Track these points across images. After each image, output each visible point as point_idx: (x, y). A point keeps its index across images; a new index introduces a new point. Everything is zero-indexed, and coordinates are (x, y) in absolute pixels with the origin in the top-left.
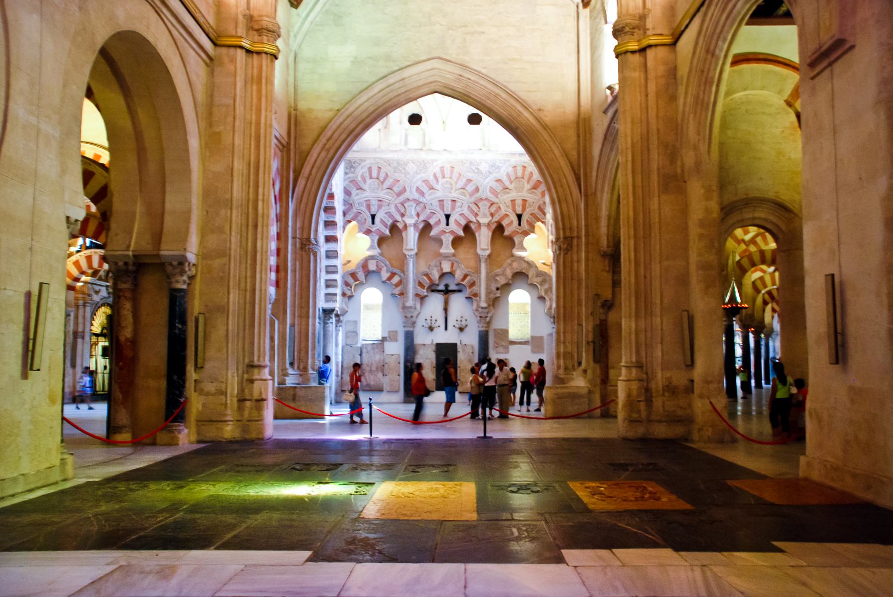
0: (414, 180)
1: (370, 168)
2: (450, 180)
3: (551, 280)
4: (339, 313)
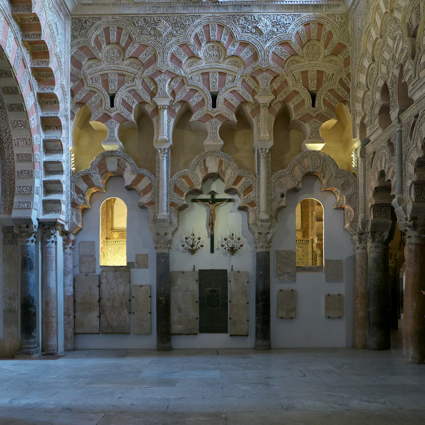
0: (168, 45)
1: (107, 30)
2: (218, 45)
3: (356, 182)
4: (67, 228)
